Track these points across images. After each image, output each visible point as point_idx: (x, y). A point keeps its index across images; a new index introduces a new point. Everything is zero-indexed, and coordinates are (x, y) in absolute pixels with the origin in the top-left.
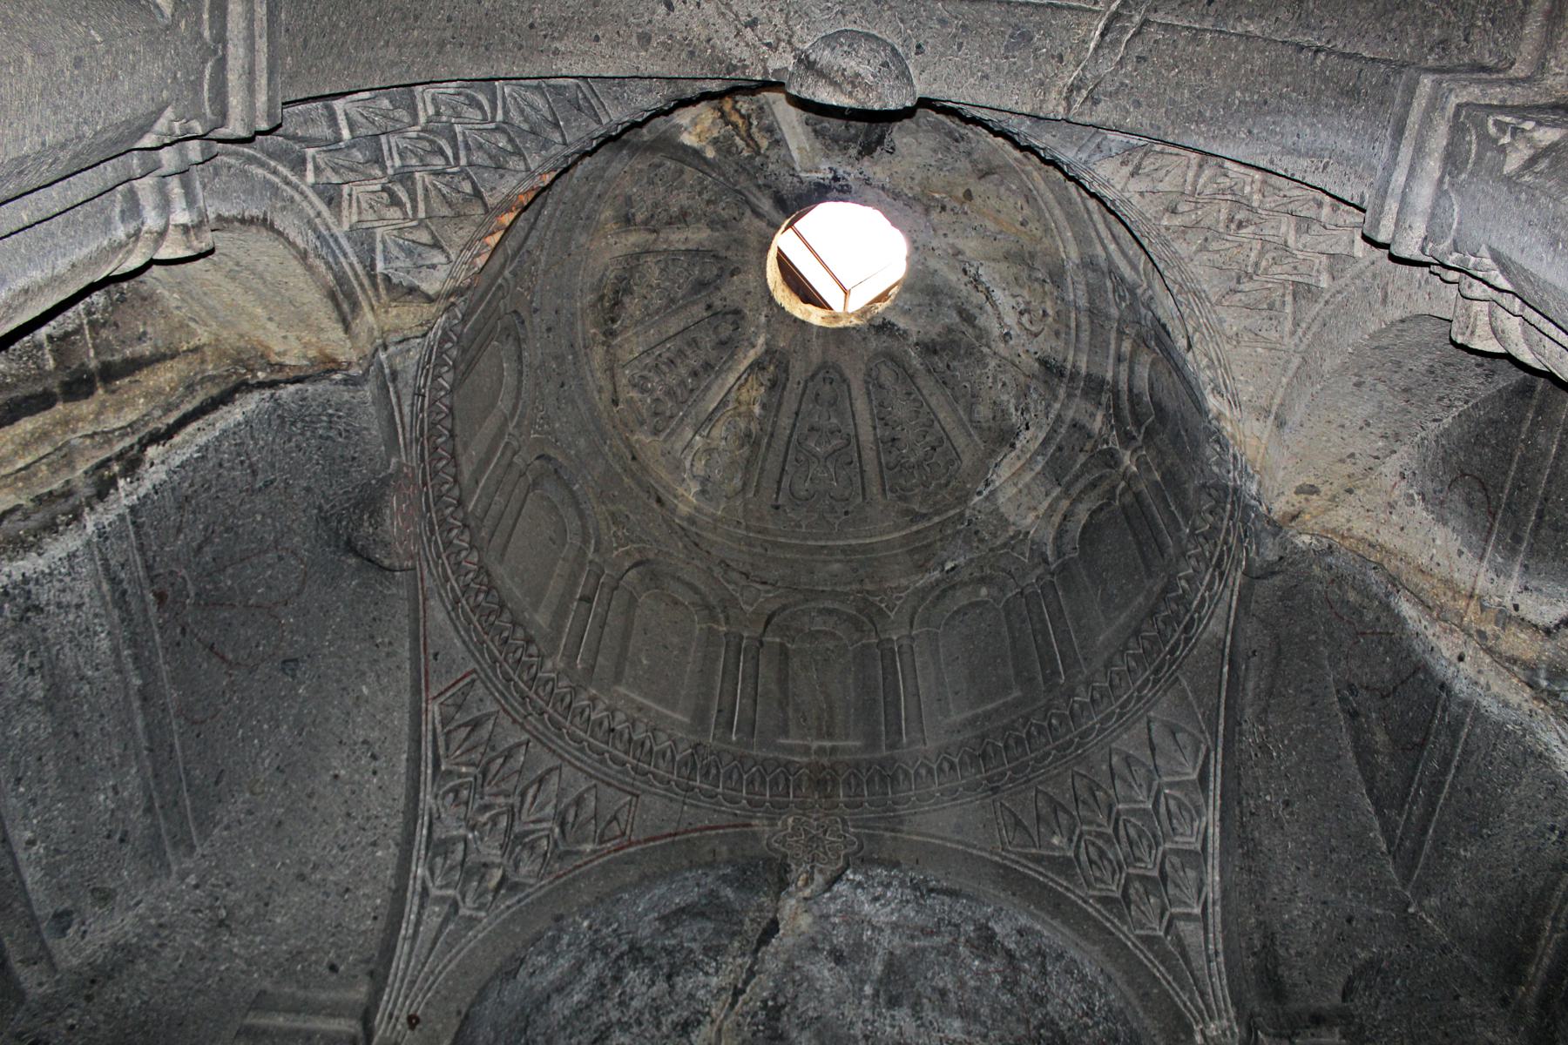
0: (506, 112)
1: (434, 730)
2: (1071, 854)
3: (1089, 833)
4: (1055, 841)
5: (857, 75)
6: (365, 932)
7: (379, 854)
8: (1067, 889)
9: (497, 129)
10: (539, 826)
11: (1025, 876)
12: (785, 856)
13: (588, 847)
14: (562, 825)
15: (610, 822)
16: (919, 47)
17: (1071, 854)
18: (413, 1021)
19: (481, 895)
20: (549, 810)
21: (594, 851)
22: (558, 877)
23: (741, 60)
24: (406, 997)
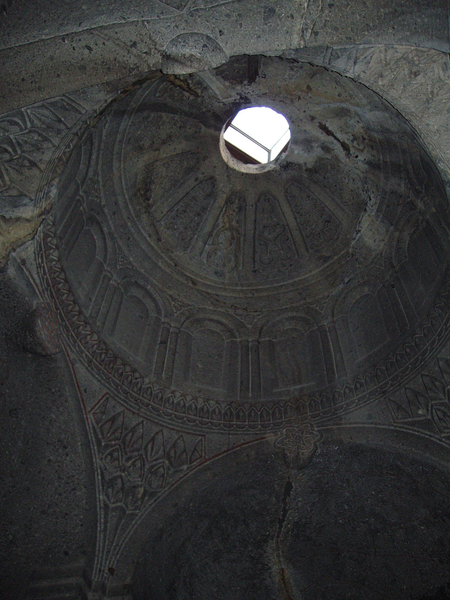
0: (32, 122)
1: (94, 427)
2: (429, 417)
3: (436, 404)
4: (420, 412)
5: (192, 55)
6: (78, 533)
7: (78, 493)
8: (430, 436)
9: (30, 132)
10: (157, 462)
11: (407, 434)
12: (284, 450)
13: (185, 467)
14: (169, 459)
15: (194, 452)
16: (220, 31)
17: (429, 417)
18: (111, 571)
19: (136, 502)
20: (161, 452)
21: (188, 468)
22: (173, 485)
23: (135, 65)
24: (106, 560)
